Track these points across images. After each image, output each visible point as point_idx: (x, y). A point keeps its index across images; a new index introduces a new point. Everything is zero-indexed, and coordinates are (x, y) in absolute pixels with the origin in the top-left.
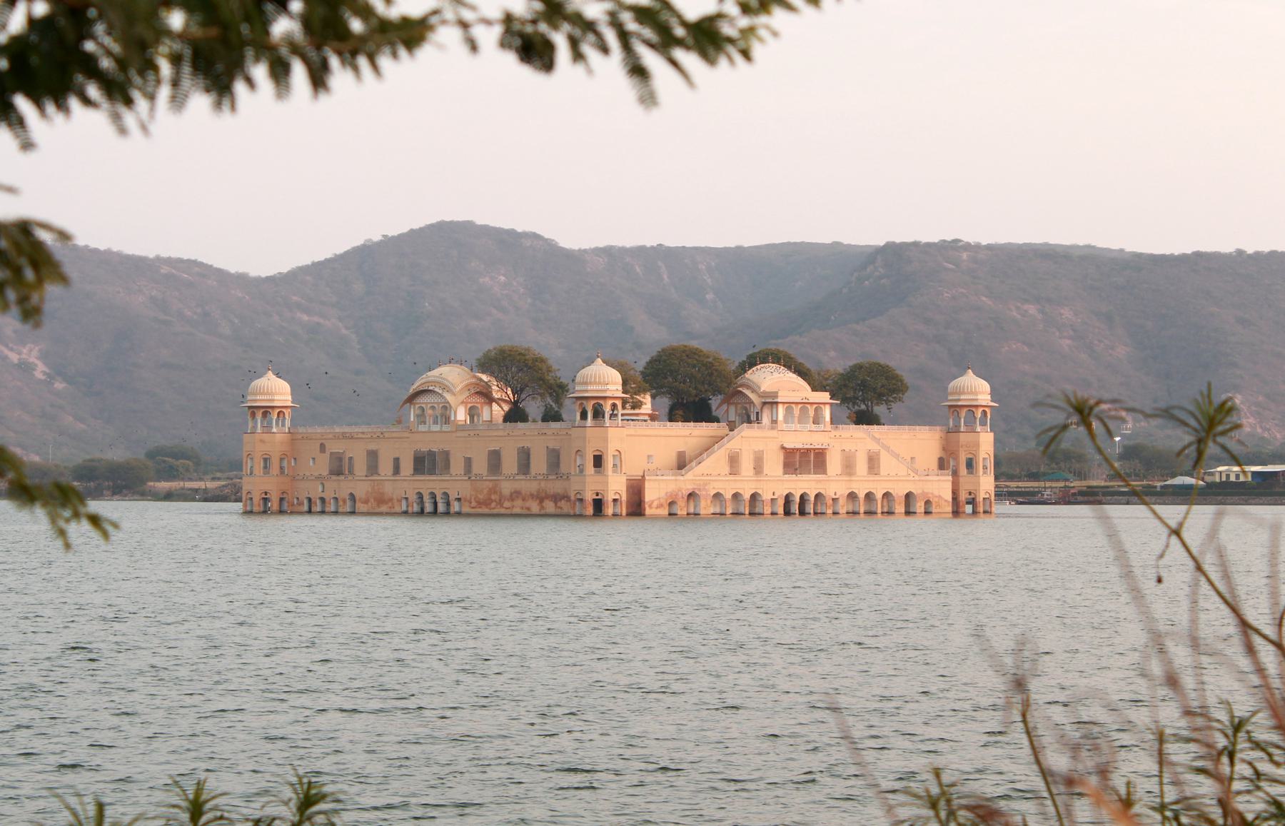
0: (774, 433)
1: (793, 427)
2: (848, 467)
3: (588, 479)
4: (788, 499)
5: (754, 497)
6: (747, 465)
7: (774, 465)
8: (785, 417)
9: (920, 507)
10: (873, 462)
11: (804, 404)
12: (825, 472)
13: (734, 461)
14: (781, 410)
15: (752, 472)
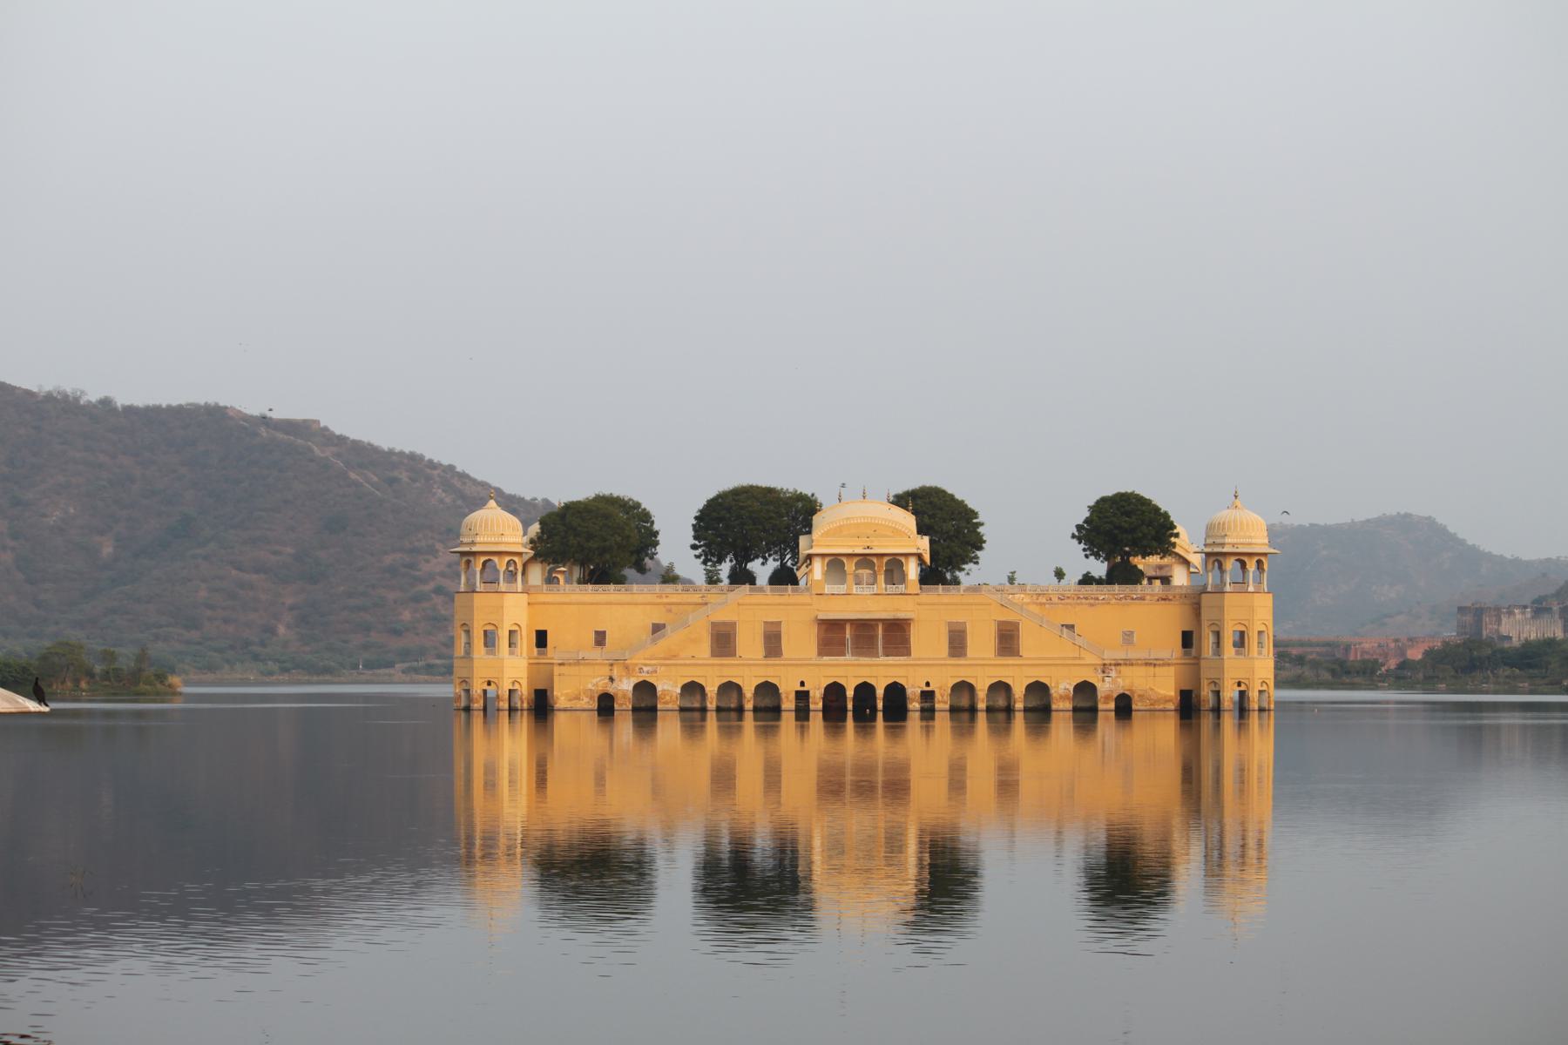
0: (803, 598)
1: (842, 589)
2: (957, 643)
3: (476, 664)
4: (834, 691)
5: (768, 690)
6: (749, 643)
7: (801, 642)
8: (826, 574)
9: (1107, 706)
10: (1007, 640)
11: (865, 560)
12: (906, 651)
13: (723, 641)
14: (818, 568)
15: (760, 651)
